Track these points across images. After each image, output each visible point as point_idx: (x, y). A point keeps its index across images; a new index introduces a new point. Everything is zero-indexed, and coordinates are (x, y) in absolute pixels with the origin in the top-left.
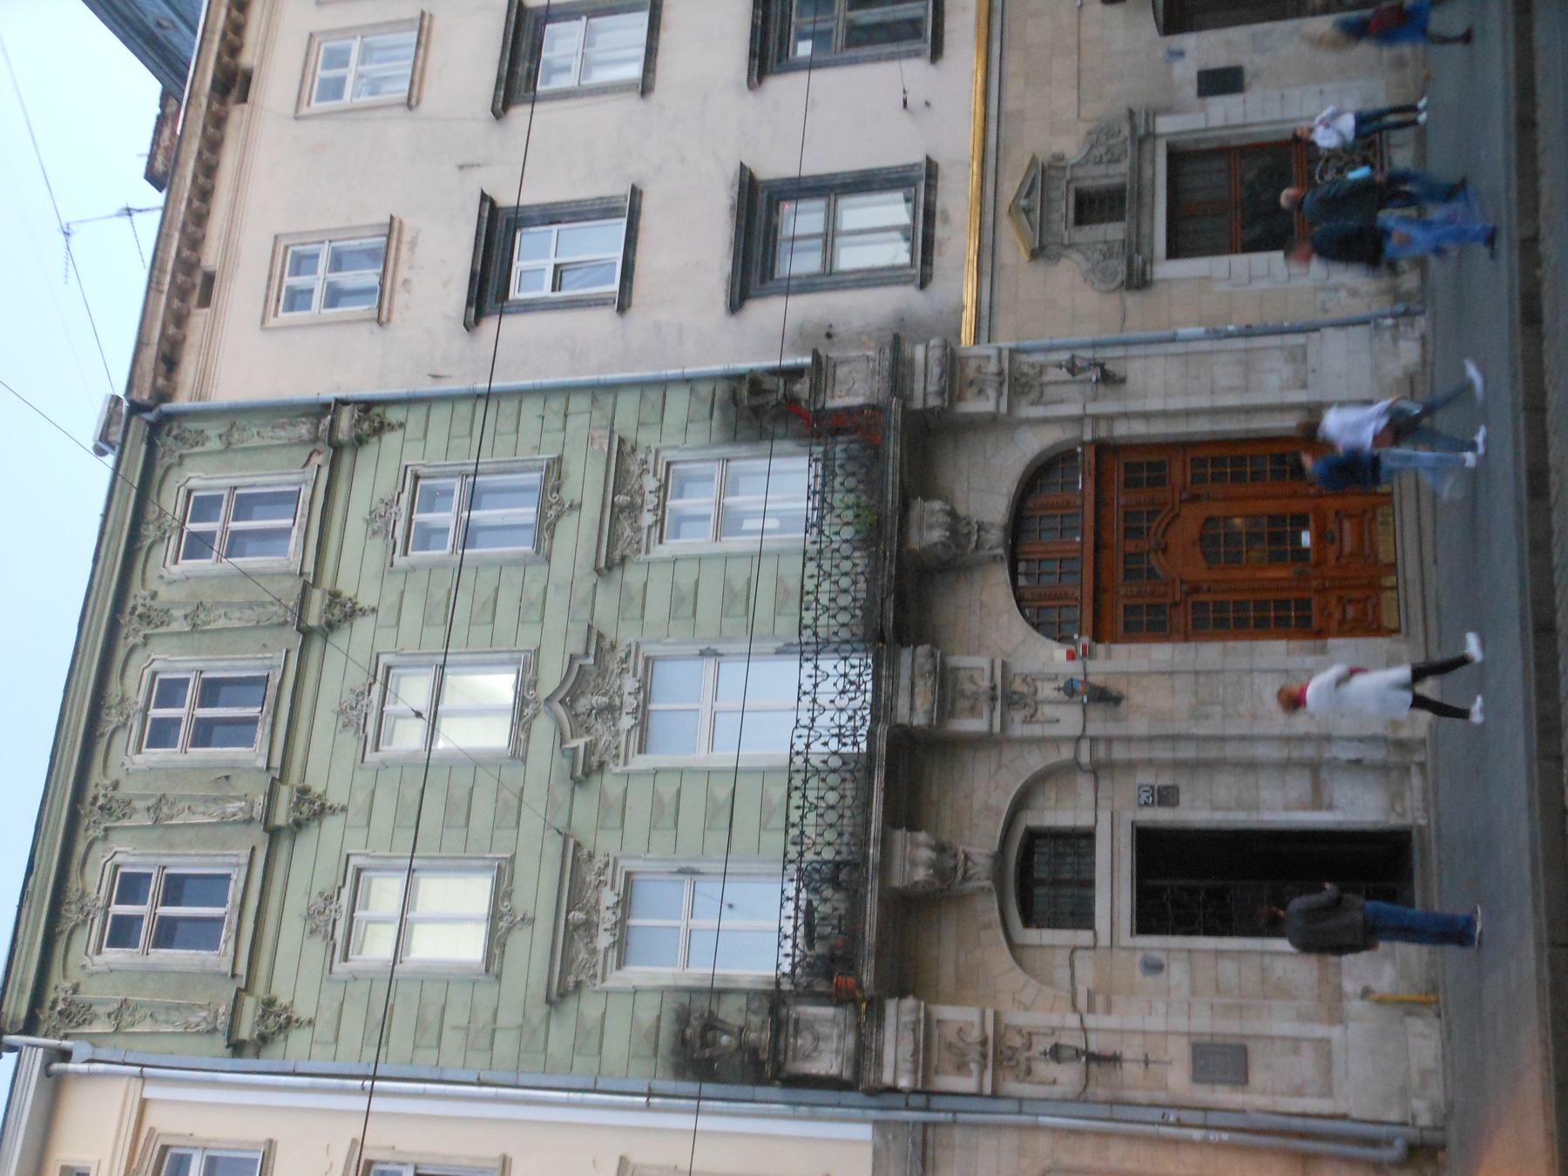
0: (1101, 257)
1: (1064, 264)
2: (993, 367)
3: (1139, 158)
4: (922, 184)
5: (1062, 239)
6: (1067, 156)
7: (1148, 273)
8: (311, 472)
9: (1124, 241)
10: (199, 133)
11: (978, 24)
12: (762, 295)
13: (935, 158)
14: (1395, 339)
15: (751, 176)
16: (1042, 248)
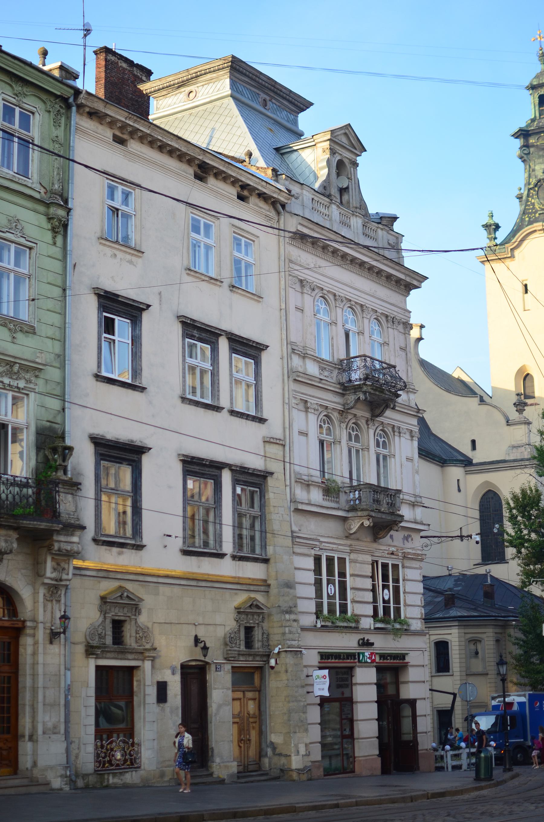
0: (99, 632)
1: (99, 613)
2: (64, 577)
3: (137, 653)
4: (133, 542)
5: (109, 613)
6: (140, 616)
7: (92, 656)
8: (38, 187)
9: (105, 644)
10: (188, 152)
11: (193, 573)
12: (96, 453)
13: (145, 549)
14: (61, 776)
15: (145, 452)
16: (105, 603)
